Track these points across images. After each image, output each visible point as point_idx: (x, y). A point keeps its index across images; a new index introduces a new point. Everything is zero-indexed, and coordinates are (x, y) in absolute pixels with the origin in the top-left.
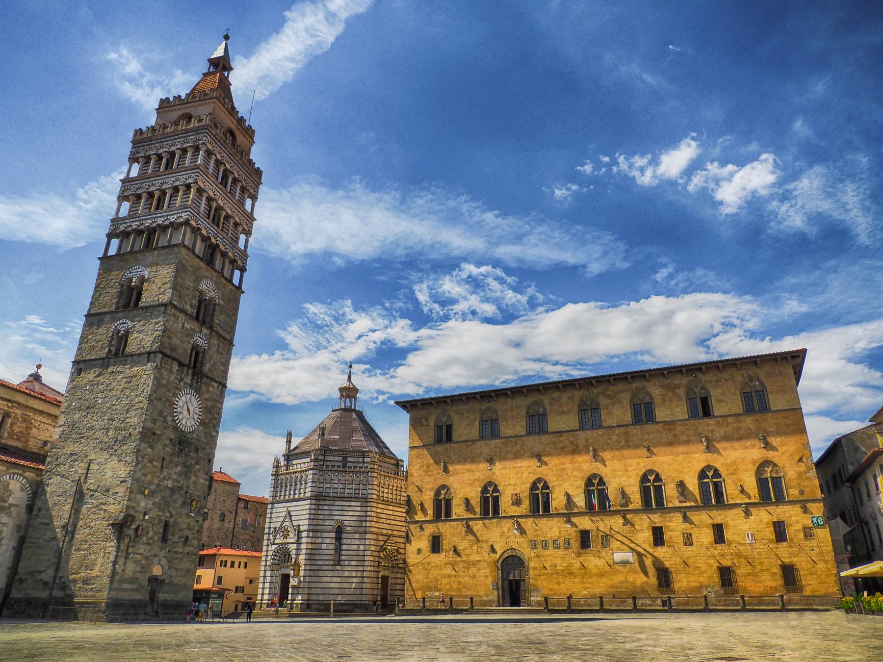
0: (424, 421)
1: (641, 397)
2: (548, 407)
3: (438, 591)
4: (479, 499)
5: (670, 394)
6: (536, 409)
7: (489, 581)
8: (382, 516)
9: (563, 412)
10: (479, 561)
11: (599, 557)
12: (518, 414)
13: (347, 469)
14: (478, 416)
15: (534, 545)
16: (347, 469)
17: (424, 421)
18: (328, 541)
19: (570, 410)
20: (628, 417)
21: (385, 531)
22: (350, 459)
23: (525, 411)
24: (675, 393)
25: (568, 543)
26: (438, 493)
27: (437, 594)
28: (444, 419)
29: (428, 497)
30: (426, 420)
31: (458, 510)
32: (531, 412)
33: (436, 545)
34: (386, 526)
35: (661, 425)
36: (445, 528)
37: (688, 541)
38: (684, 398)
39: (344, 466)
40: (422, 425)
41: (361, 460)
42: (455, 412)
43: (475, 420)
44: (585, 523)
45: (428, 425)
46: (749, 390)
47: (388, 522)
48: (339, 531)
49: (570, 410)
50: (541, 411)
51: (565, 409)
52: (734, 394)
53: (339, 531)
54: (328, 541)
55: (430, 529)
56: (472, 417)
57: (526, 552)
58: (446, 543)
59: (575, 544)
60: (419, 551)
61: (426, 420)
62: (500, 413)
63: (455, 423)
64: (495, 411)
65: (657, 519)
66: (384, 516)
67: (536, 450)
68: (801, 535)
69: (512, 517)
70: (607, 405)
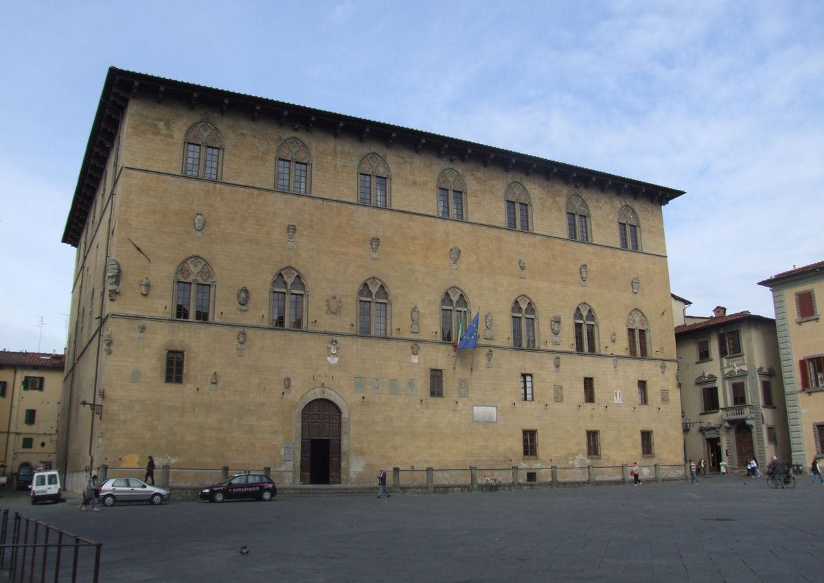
1: (517, 193)
3: (174, 455)
4: (267, 295)
5: (550, 201)
9: (415, 183)
10: (262, 405)
11: (454, 410)
14: (274, 147)
17: (161, 125)
19: (425, 184)
24: (555, 201)
26: (182, 269)
27: (173, 461)
29: (163, 273)
30: (168, 125)
31: (223, 306)
33: (174, 367)
35: (538, 238)
36: (191, 337)
37: (559, 398)
38: (564, 210)
40: (157, 132)
45: (171, 136)
46: (625, 222)
50: (381, 171)
51: (420, 179)
52: (612, 221)
55: (163, 336)
57: (344, 397)
60: (136, 376)
67: (373, 233)
68: (659, 399)
69: (325, 333)
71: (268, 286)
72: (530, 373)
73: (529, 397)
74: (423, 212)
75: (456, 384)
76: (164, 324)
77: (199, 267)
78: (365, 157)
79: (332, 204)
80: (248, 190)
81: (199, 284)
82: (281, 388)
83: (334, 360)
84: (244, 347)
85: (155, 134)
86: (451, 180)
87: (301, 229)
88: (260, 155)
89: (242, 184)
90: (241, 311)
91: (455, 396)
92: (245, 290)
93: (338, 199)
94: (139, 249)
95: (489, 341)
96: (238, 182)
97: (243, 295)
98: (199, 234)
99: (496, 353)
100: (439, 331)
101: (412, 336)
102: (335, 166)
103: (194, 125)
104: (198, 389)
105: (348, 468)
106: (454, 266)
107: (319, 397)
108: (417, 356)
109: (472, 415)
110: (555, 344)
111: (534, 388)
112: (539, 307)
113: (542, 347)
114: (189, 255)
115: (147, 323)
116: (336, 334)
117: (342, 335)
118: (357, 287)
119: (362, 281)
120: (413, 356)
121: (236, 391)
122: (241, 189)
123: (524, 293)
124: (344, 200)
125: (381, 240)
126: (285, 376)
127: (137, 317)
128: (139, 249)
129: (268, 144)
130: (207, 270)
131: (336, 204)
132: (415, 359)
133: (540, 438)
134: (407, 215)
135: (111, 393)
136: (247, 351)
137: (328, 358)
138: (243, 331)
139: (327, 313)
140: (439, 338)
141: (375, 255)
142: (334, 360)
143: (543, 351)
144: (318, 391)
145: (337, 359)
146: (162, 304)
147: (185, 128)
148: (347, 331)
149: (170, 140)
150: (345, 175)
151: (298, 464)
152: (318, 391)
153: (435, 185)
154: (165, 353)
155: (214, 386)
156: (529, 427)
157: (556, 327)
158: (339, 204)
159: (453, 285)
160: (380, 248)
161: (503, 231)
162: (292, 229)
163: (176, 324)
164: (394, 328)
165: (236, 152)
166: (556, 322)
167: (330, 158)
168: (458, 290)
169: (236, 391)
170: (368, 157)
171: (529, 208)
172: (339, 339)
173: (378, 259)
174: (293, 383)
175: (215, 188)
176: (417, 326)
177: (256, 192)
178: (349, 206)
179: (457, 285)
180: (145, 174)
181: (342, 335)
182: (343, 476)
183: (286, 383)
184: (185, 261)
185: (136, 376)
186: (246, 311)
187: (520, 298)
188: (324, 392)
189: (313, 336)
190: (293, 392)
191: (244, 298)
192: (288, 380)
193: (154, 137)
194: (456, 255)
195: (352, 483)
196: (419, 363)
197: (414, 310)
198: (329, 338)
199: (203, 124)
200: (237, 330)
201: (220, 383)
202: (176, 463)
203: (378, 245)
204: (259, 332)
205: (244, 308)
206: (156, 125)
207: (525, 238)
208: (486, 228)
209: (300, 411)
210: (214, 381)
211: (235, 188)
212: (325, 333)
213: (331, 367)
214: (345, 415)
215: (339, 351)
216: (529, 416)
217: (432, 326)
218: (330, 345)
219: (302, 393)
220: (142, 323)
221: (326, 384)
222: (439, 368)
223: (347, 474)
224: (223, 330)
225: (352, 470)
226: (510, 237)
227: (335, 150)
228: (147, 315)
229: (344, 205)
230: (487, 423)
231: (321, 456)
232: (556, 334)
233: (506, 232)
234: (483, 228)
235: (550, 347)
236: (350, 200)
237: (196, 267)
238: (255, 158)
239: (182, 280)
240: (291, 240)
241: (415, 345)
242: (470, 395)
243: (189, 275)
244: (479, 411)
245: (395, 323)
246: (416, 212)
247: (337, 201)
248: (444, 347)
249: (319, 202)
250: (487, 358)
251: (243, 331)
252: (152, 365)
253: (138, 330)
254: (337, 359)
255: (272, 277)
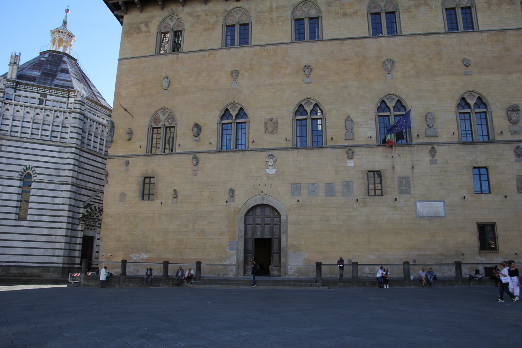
0: (143, 26)
2: (324, 8)
3: (147, 252)
4: (215, 126)
6: (306, 10)
7: (225, 239)
8: (86, 166)
9: (345, 15)
11: (395, 207)
12: (280, 16)
13: (44, 106)
14: (221, 19)
15: (296, 188)
16: (44, 106)
17: (143, 26)
18: (12, 190)
19: (355, 13)
20: (439, 22)
21: (90, 185)
22: (49, 97)
23: (289, 13)
25: (347, 185)
26: (155, 119)
27: (146, 256)
28: (172, 24)
30: (147, 25)
31: (184, 140)
32: (299, 14)
33: (147, 188)
34: (92, 180)
36: (161, 166)
39: (41, 102)
41: (65, 100)
42: (188, 14)
43: (216, 22)
44: (378, 159)
45: (148, 31)
47: (96, 175)
48: (27, 178)
49: (355, 13)
51: (349, 11)
53: (27, 178)
54: (12, 190)
55: (139, 168)
56: (213, 20)
57: (282, 199)
58: (163, 189)
59: (359, 188)
60: (123, 195)
61: (147, 25)
62: (253, 15)
63: (187, 27)
64: (246, 12)
65: (480, 155)
66: (90, 168)
67: (305, 62)
69: (263, 150)
70: (410, 7)
71: (217, 119)
72: (484, 165)
73: (485, 189)
74: (355, 36)
75: (396, 183)
76: (141, 159)
77: (167, 115)
78: (298, 6)
79: (269, 48)
80: (201, 53)
81: (167, 127)
82: (226, 197)
83: (272, 171)
84: (196, 168)
85: (138, 33)
86: (382, 4)
87: (243, 72)
88: (210, 26)
89: (197, 49)
90: (196, 141)
91: (396, 194)
92: (197, 125)
93: (274, 42)
94: (126, 110)
95: (432, 139)
96: (194, 50)
97: (195, 129)
98: (166, 92)
99: (440, 150)
100: (374, 136)
101: (346, 143)
102: (271, 19)
103: (164, 19)
104: (161, 203)
105: (286, 263)
106: (389, 76)
107: (259, 203)
108: (352, 161)
109: (416, 211)
110: (513, 133)
111: (491, 180)
112: (490, 100)
113: (498, 138)
114: (158, 108)
115: (130, 159)
116: (273, 149)
117: (278, 149)
118: (292, 108)
119: (296, 103)
120: (349, 161)
121: (191, 203)
122: (196, 54)
123: (470, 89)
124: (280, 42)
125: (313, 66)
126: (229, 187)
127: (124, 156)
128: (126, 110)
129: (217, 17)
130: (172, 118)
131: (272, 47)
132: (351, 163)
133: (500, 231)
134: (339, 42)
135: (107, 210)
136: (200, 172)
137: (267, 170)
138: (195, 157)
139: (266, 133)
140: (374, 140)
141: (308, 80)
142: (272, 171)
143: (499, 142)
144: (258, 197)
145: (275, 170)
146: (140, 143)
147: (158, 23)
148: (284, 146)
149: (148, 34)
150: (280, 23)
151: (242, 258)
152: (258, 197)
153: (365, 11)
154: (141, 179)
155: (175, 200)
156: (485, 219)
157: (514, 116)
158: (275, 47)
159: (388, 93)
160: (313, 73)
161: (441, 36)
162: (235, 73)
163: (149, 158)
164: (329, 138)
165: (192, 29)
166: (513, 111)
167: (267, 14)
168: (394, 97)
169: (191, 203)
170: (301, 5)
171: (473, 10)
172: (275, 153)
173: (311, 83)
174: (236, 193)
175: (177, 58)
176: (351, 134)
177: (207, 53)
178: (283, 46)
179: (393, 92)
180: (131, 60)
181: (278, 149)
182: (282, 269)
183: (231, 194)
184: (156, 113)
185: (123, 195)
186: (199, 140)
187: (468, 94)
188: (263, 199)
189: (254, 153)
190: (236, 200)
191: (198, 128)
192: (232, 191)
193: (138, 35)
194: (389, 65)
195: (291, 275)
196: (355, 166)
197: (347, 120)
198: (267, 153)
199: (170, 17)
200: (192, 155)
201: (179, 198)
202: (147, 259)
203: (311, 71)
204: (208, 155)
205: (197, 139)
206: (139, 27)
207: (468, 37)
208: (423, 37)
209: (243, 216)
210: (175, 196)
211: (192, 54)
212: (263, 150)
213: (269, 176)
214: (283, 217)
215: (277, 163)
216: (487, 209)
217: (367, 129)
218: (267, 159)
219: (244, 200)
220: (126, 159)
221: (265, 192)
222: (377, 169)
223: (286, 268)
224: (182, 157)
225: (290, 264)
226: (452, 39)
227: (271, 8)
228: (130, 154)
229: (279, 46)
230: (432, 218)
231: (263, 251)
232: (515, 123)
233: (446, 36)
234: (419, 37)
235: (507, 137)
236: (285, 41)
237: (164, 115)
238: (206, 30)
239: (155, 126)
240: (235, 82)
241: (350, 151)
242: (412, 192)
243: (159, 122)
244: (422, 208)
245: (330, 133)
246: (348, 37)
247: (273, 44)
248: (381, 149)
249: (258, 48)
250: (429, 155)
251: (195, 157)
252: (133, 188)
253: (124, 165)
254: (275, 170)
255: (219, 112)
